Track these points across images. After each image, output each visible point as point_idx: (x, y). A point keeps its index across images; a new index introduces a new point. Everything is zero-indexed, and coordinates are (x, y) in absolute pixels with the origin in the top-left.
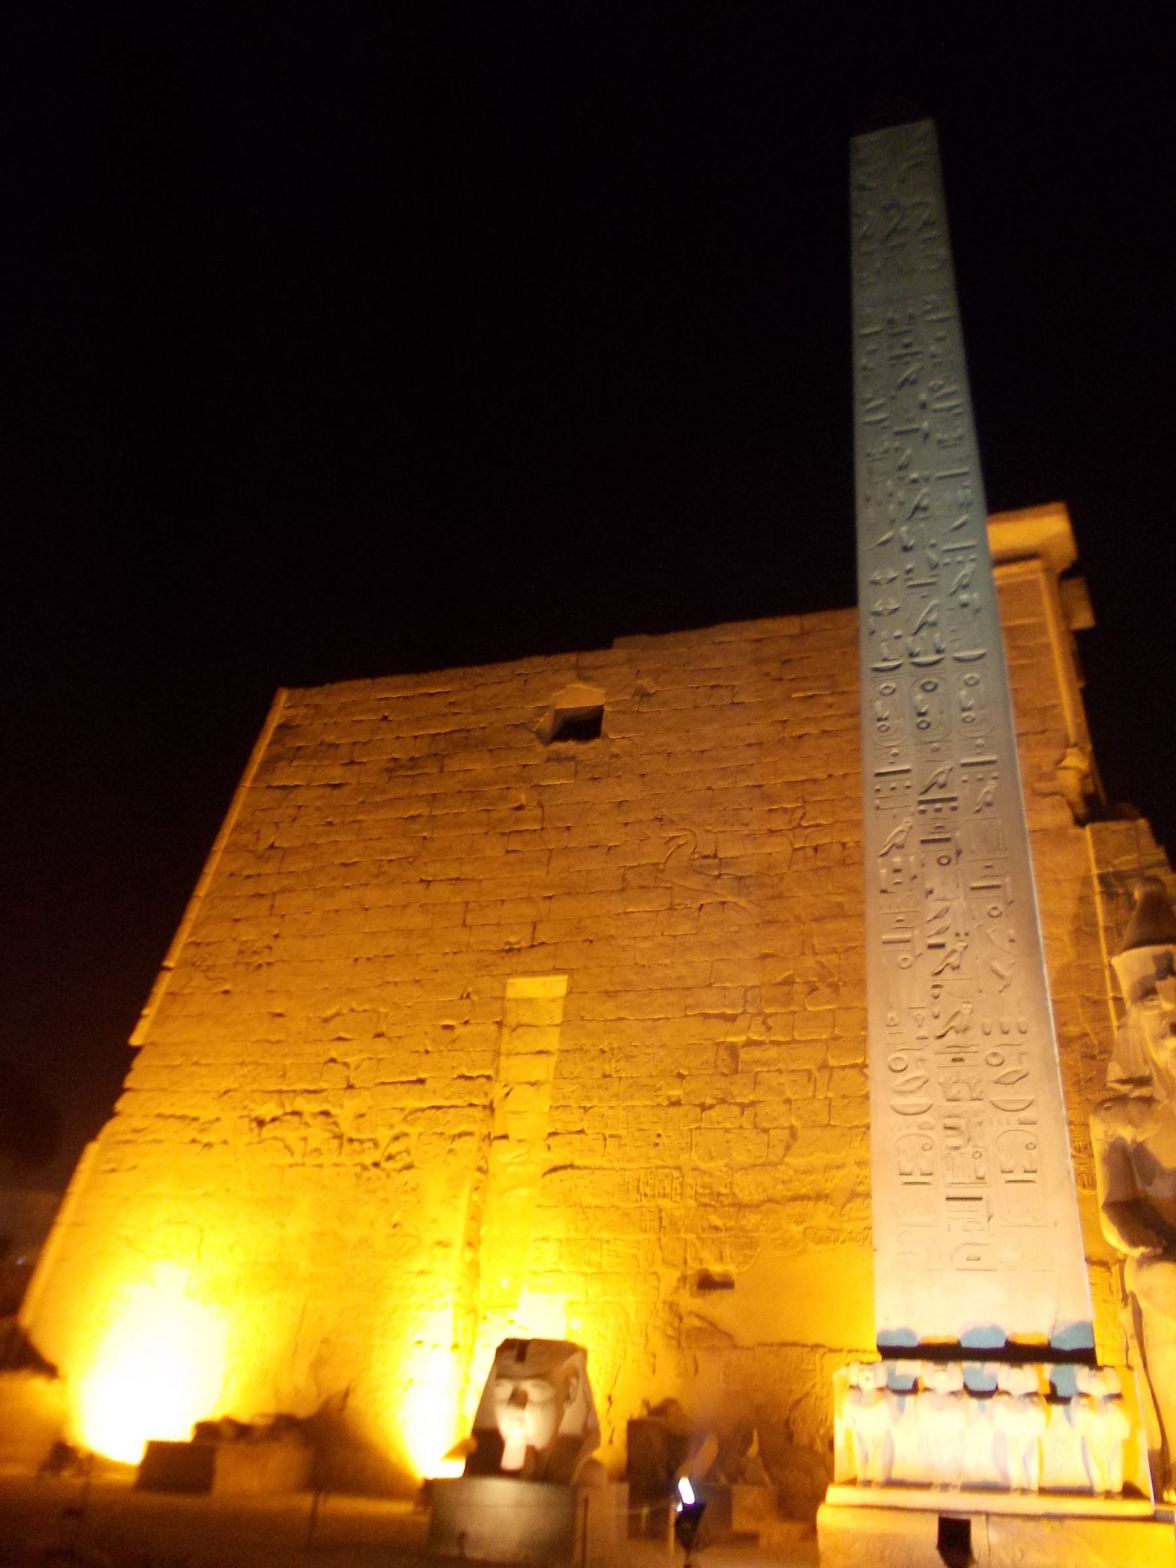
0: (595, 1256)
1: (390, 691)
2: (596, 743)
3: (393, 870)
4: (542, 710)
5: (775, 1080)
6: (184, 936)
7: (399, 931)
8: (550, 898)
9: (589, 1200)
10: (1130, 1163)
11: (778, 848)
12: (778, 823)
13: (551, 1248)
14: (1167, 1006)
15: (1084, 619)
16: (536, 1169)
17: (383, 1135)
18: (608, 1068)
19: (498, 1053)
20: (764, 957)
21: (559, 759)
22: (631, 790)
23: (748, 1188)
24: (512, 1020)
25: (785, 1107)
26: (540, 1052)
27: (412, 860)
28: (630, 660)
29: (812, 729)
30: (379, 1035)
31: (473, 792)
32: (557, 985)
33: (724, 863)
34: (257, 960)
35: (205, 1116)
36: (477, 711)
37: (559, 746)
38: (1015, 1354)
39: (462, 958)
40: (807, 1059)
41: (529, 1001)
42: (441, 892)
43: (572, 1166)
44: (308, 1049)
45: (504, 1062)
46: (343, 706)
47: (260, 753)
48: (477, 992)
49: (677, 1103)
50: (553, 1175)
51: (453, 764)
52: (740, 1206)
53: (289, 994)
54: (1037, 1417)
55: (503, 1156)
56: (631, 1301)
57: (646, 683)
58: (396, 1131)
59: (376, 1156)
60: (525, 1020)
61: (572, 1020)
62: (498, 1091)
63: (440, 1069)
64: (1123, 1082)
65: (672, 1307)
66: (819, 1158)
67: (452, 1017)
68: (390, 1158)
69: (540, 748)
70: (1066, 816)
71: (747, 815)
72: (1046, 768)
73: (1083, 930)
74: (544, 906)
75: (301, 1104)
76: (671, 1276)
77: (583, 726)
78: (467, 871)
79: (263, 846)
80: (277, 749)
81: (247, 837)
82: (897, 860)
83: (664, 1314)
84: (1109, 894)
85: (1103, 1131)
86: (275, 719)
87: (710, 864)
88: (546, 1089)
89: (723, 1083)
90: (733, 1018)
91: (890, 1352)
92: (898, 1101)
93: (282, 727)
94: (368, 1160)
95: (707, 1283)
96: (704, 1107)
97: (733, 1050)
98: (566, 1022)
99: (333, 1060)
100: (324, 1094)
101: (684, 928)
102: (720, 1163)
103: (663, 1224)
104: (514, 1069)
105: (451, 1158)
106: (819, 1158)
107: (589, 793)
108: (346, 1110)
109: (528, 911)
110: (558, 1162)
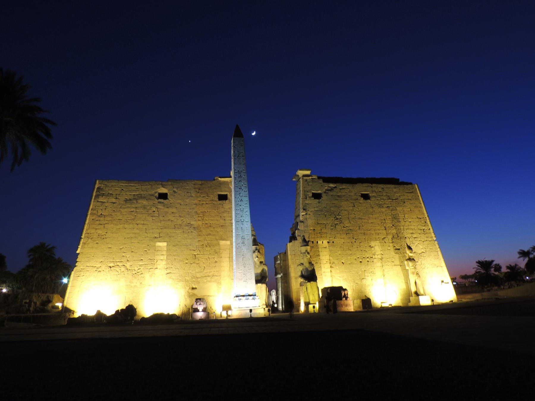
1: (123, 184)
2: (167, 200)
3: (130, 221)
4: (156, 193)
7: (133, 233)
11: (200, 223)
21: (160, 203)
22: (174, 210)
23: (198, 275)
24: (157, 249)
27: (133, 219)
28: (172, 185)
29: (205, 203)
31: (144, 207)
32: (165, 244)
33: (191, 225)
34: (103, 237)
35: (97, 266)
37: (160, 200)
39: (146, 239)
40: (206, 257)
41: (160, 246)
42: (140, 226)
51: (139, 201)
57: (175, 189)
65: (188, 292)
66: (208, 271)
69: (156, 200)
71: (194, 217)
75: (118, 264)
76: (188, 288)
77: (163, 196)
78: (145, 222)
79: (99, 214)
80: (98, 193)
81: (95, 212)
86: (96, 186)
87: (189, 225)
93: (98, 188)
94: (134, 273)
95: (193, 289)
97: (195, 255)
98: (167, 250)
101: (186, 235)
103: (186, 281)
106: (208, 271)
107: (166, 210)
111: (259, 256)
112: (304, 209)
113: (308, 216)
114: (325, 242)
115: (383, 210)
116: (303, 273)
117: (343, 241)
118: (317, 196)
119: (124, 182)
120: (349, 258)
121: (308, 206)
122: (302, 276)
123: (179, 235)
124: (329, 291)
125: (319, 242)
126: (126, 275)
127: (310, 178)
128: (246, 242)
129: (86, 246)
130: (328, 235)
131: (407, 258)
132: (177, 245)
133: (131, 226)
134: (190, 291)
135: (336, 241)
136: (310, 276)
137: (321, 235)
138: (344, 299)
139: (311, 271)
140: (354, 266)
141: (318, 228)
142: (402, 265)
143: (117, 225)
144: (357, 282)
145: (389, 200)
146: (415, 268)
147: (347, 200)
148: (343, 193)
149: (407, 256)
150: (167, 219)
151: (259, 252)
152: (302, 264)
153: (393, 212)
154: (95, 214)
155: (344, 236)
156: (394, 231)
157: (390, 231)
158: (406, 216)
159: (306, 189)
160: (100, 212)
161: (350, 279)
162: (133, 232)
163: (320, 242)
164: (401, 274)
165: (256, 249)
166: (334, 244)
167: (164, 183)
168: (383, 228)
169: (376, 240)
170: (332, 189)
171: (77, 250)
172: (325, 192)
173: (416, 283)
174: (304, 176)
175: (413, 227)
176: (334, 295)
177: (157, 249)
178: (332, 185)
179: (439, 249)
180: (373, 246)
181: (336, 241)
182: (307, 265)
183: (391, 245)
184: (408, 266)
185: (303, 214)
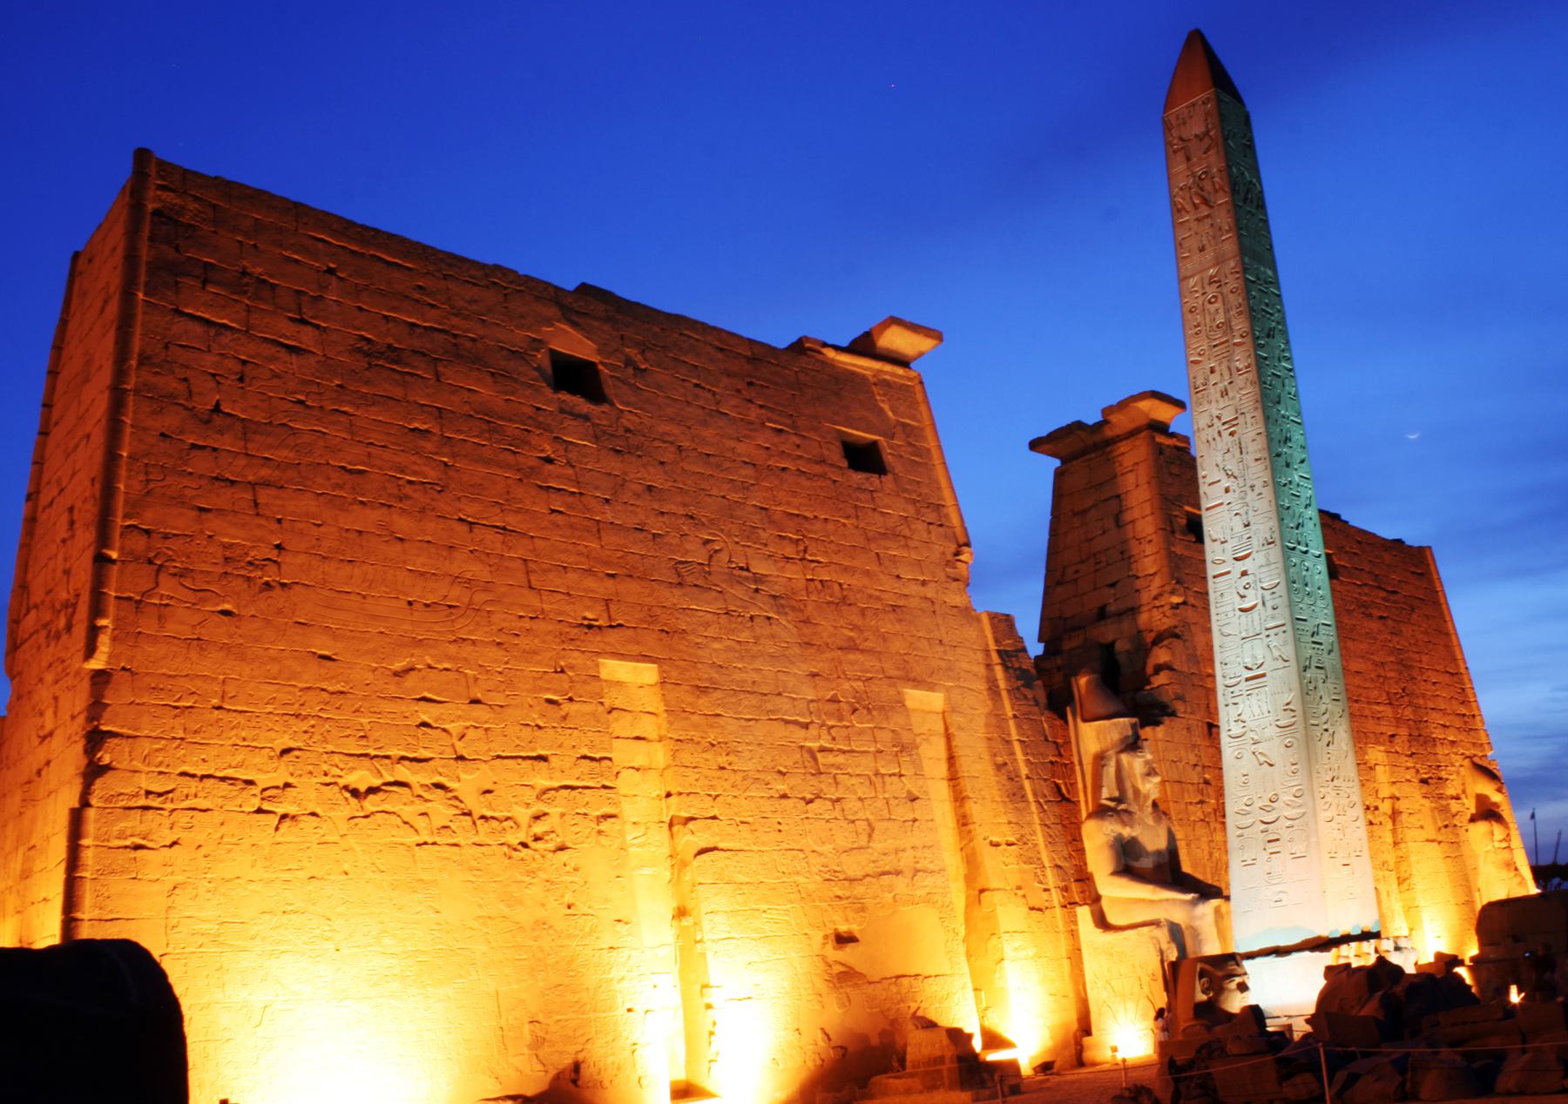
8: (613, 576)
9: (741, 878)
12: (790, 551)
14: (1149, 757)
17: (523, 814)
20: (814, 675)
25: (859, 804)
26: (638, 738)
30: (476, 701)
33: (758, 579)
39: (540, 626)
43: (715, 849)
48: (572, 668)
50: (703, 856)
58: (534, 810)
60: (617, 704)
63: (560, 746)
64: (1111, 799)
67: (555, 692)
68: (537, 839)
72: (949, 557)
99: (424, 724)
100: (431, 763)
103: (806, 897)
105: (602, 840)
106: (890, 844)
110: (704, 845)
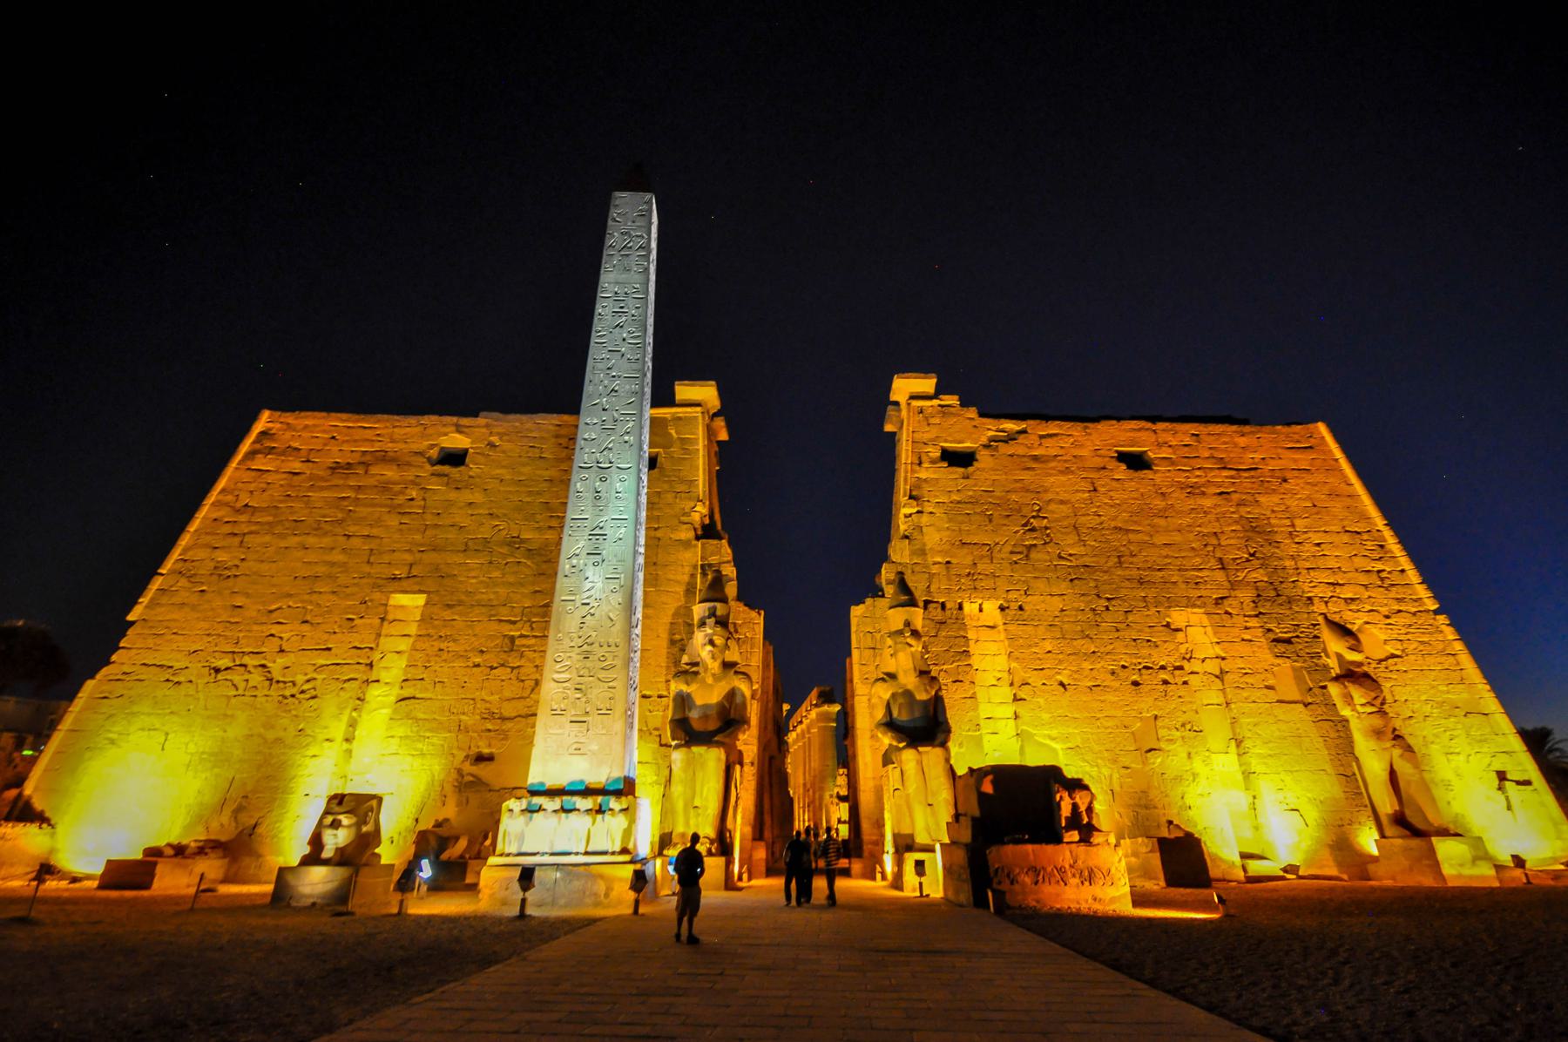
0: (420, 746)
2: (462, 468)
3: (328, 527)
5: (531, 655)
6: (175, 554)
9: (421, 716)
10: (683, 701)
13: (396, 741)
14: (709, 631)
15: (723, 436)
16: (393, 699)
18: (443, 646)
19: (379, 635)
22: (478, 497)
23: (508, 710)
24: (390, 617)
28: (487, 426)
32: (420, 600)
33: (523, 541)
35: (177, 665)
36: (393, 441)
38: (588, 792)
44: (255, 628)
45: (382, 640)
46: (306, 427)
47: (245, 447)
49: (478, 666)
51: (373, 470)
52: (504, 719)
53: (247, 595)
54: (588, 819)
55: (374, 692)
56: (437, 768)
59: (294, 691)
61: (426, 619)
62: (376, 656)
65: (459, 772)
69: (428, 467)
70: (691, 534)
73: (690, 590)
74: (418, 556)
75: (247, 660)
76: (461, 755)
77: (455, 458)
78: (375, 532)
80: (258, 446)
81: (230, 498)
82: (574, 561)
83: (454, 775)
84: (704, 574)
85: (677, 686)
86: (259, 427)
88: (405, 656)
89: (504, 656)
90: (514, 623)
91: (534, 793)
92: (556, 676)
93: (263, 433)
94: (287, 693)
95: (481, 759)
96: (492, 668)
97: (512, 639)
98: (422, 620)
101: (496, 574)
102: (496, 697)
103: (461, 728)
104: (386, 643)
107: (453, 495)
108: (276, 666)
109: (408, 558)
111: (719, 641)
112: (911, 497)
113: (925, 519)
114: (991, 607)
115: (1207, 503)
116: (895, 714)
117: (1057, 603)
118: (959, 459)
119: (344, 416)
120: (1087, 665)
121: (926, 487)
122: (890, 725)
123: (473, 574)
124: (988, 788)
125: (967, 606)
126: (261, 699)
127: (935, 402)
128: (608, 549)
129: (164, 600)
130: (1002, 585)
131: (1336, 671)
132: (460, 603)
133: (327, 541)
134: (468, 768)
135: (1031, 603)
136: (924, 726)
137: (974, 581)
138: (1074, 836)
139: (925, 703)
140: (1111, 697)
141: (963, 559)
142: (1313, 698)
143: (282, 536)
144: (1126, 761)
145: (1226, 473)
146: (1382, 712)
147: (1067, 471)
148: (1050, 447)
149: (1333, 663)
150: (448, 522)
151: (723, 623)
152: (892, 676)
153: (1243, 510)
154: (227, 504)
155: (1064, 587)
156: (1260, 575)
157: (1241, 575)
158: (1298, 522)
159: (918, 436)
160: (245, 499)
161: (1096, 748)
162: (328, 558)
163: (970, 608)
164: (1314, 739)
165: (713, 614)
166: (1025, 615)
167: (465, 421)
168: (1213, 563)
169: (1190, 603)
170: (1010, 438)
171: (129, 611)
172: (986, 446)
173: (1393, 775)
174: (913, 397)
175: (1332, 564)
176: (1018, 810)
177: (390, 617)
178: (1011, 426)
179: (1459, 646)
180: (1182, 625)
181: (1031, 603)
182: (909, 680)
183: (1253, 623)
184: (1349, 700)
185: (907, 511)
